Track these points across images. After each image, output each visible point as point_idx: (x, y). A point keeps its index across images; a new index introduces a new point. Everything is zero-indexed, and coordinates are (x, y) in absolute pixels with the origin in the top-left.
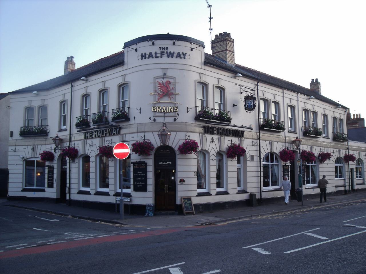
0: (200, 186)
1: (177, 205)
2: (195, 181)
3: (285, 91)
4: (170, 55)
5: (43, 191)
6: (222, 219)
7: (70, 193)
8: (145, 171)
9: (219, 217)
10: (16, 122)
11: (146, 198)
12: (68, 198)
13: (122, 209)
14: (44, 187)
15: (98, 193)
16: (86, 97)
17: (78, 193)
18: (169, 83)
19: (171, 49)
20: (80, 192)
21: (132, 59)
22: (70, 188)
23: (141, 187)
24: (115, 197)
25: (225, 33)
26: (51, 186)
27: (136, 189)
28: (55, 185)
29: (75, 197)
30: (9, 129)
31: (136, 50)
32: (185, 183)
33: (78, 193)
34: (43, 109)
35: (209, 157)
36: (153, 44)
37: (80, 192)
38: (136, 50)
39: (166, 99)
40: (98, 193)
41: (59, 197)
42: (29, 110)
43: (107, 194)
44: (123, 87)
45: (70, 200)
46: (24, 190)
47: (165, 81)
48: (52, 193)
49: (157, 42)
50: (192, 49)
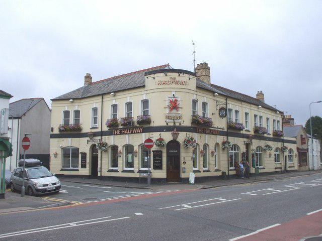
4: (177, 83)
5: (78, 170)
6: (209, 186)
7: (101, 171)
8: (161, 156)
10: (57, 121)
11: (161, 174)
12: (99, 175)
13: (149, 181)
15: (124, 171)
16: (115, 107)
18: (176, 100)
19: (178, 79)
20: (110, 171)
23: (158, 166)
26: (84, 166)
27: (155, 168)
28: (88, 166)
29: (105, 173)
31: (154, 78)
34: (77, 113)
35: (209, 148)
36: (166, 75)
37: (110, 171)
38: (154, 78)
39: (174, 111)
40: (124, 171)
41: (90, 174)
42: (67, 114)
43: (117, 171)
44: (145, 103)
45: (101, 176)
46: (62, 170)
47: (174, 99)
48: (86, 172)
49: (169, 74)
50: (190, 79)
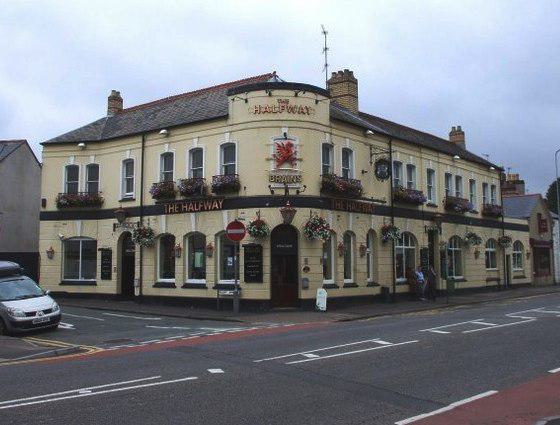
0: (347, 276)
1: (301, 299)
2: (320, 269)
3: (440, 155)
4: (292, 110)
5: (94, 284)
6: (356, 316)
7: (141, 286)
8: (260, 256)
9: (355, 313)
10: (53, 186)
11: (260, 291)
12: (137, 293)
13: (236, 305)
14: (94, 277)
15: (186, 286)
16: (168, 158)
17: (154, 286)
18: (290, 145)
19: (293, 102)
20: (157, 285)
21: (238, 107)
22: (141, 280)
23: (254, 276)
24: (216, 291)
25: (347, 71)
26: (106, 276)
27: (248, 279)
28: (114, 275)
29: (149, 290)
30: (40, 194)
31: (246, 101)
32: (311, 271)
33: (154, 286)
34: (93, 170)
35: (354, 240)
36: (270, 95)
37: (157, 285)
38: (246, 101)
39: (286, 167)
40: (186, 286)
41: (120, 292)
42: (72, 171)
43: (172, 286)
44: (229, 150)
45: (141, 295)
46: (63, 283)
47: (285, 142)
48: (110, 287)
49: (275, 92)
50: (317, 102)
